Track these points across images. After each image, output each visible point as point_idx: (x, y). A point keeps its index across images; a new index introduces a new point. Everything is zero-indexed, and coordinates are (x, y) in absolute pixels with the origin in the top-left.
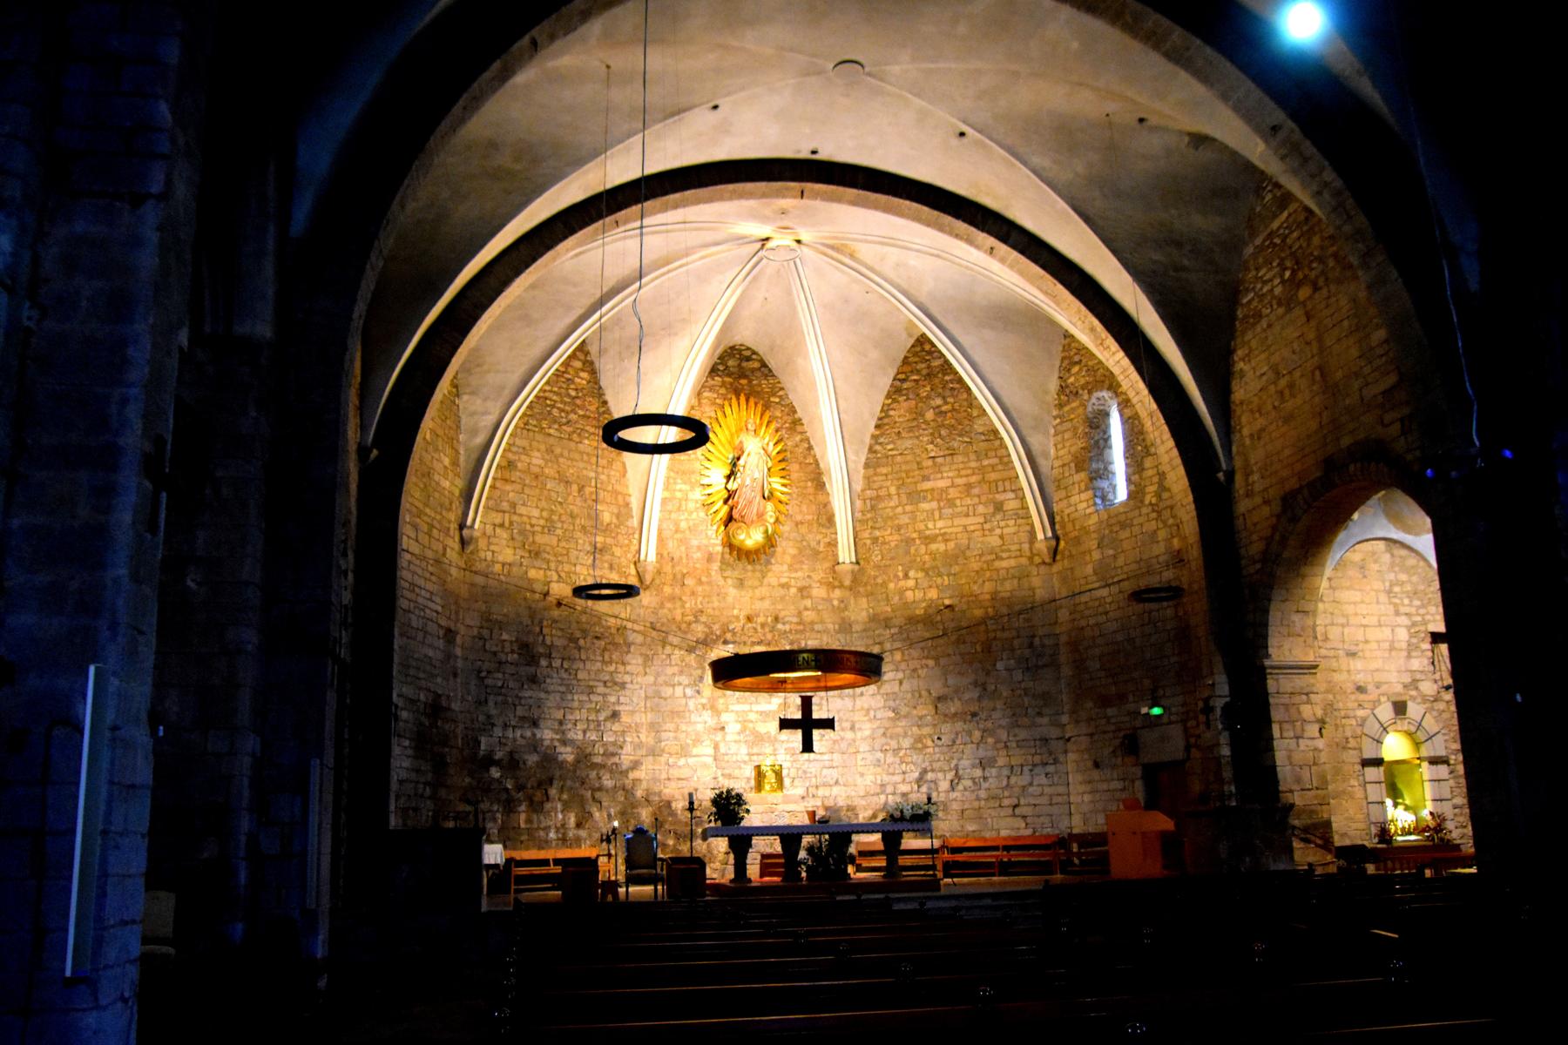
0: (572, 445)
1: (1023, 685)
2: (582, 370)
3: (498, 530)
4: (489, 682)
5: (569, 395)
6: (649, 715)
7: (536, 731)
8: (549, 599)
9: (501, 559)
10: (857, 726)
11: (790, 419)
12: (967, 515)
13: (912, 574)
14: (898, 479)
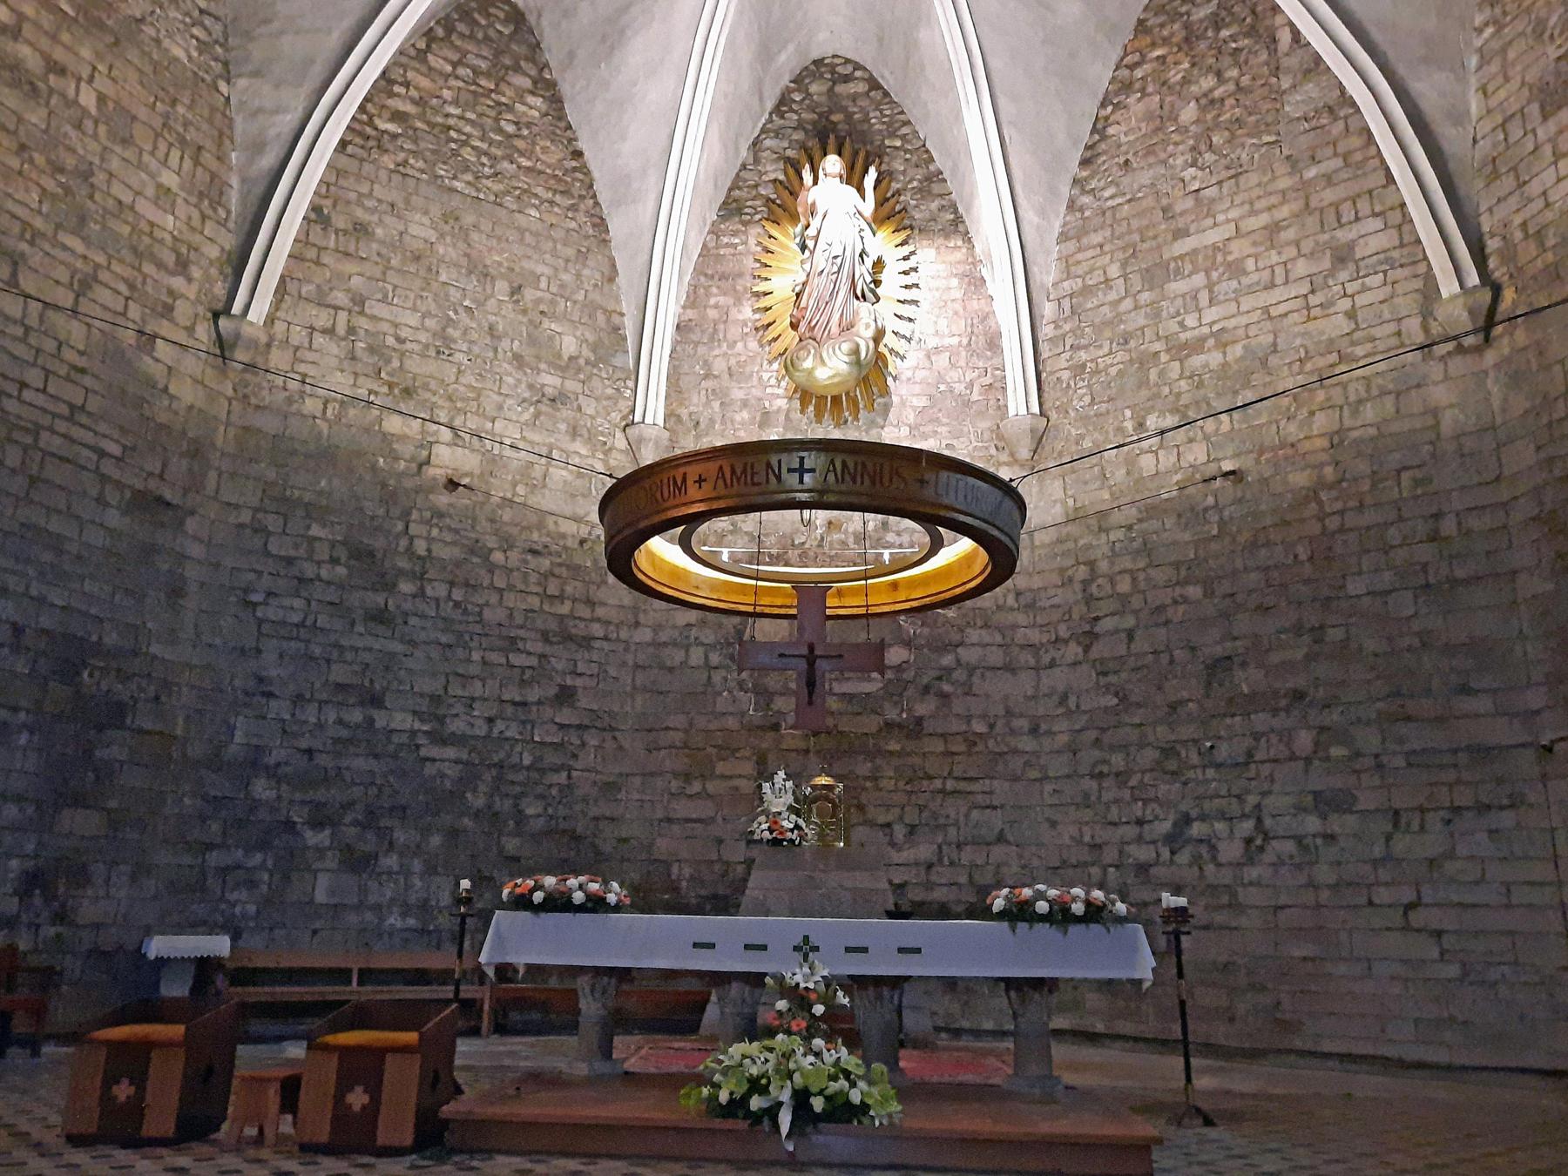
1: (1416, 626)
2: (532, 93)
3: (319, 340)
4: (271, 612)
5: (500, 131)
6: (639, 700)
8: (431, 471)
10: (1044, 727)
11: (919, 174)
12: (1272, 285)
14: (1124, 249)
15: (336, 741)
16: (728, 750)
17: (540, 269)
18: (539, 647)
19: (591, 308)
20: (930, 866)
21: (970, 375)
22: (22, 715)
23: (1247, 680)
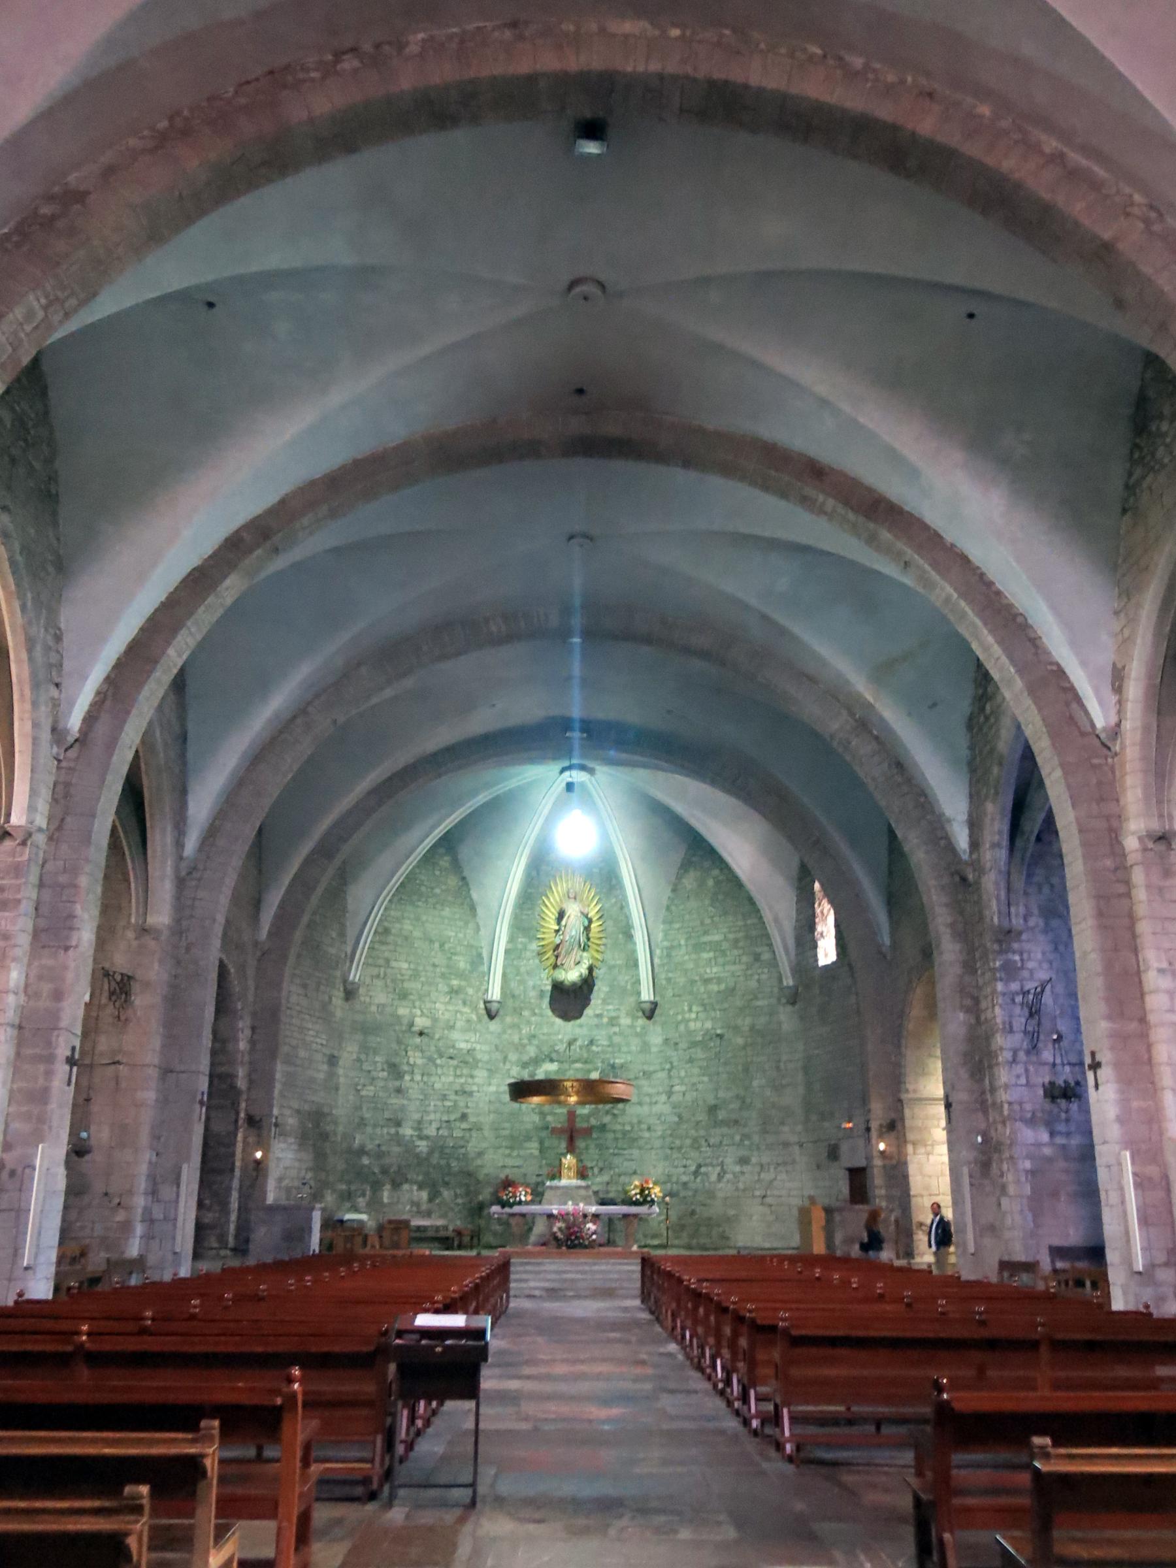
4: (363, 1093)
9: (377, 1001)
12: (735, 963)
13: (695, 1008)
16: (528, 1138)
18: (453, 1097)
19: (470, 946)
20: (608, 1183)
21: (627, 978)
23: (722, 1115)
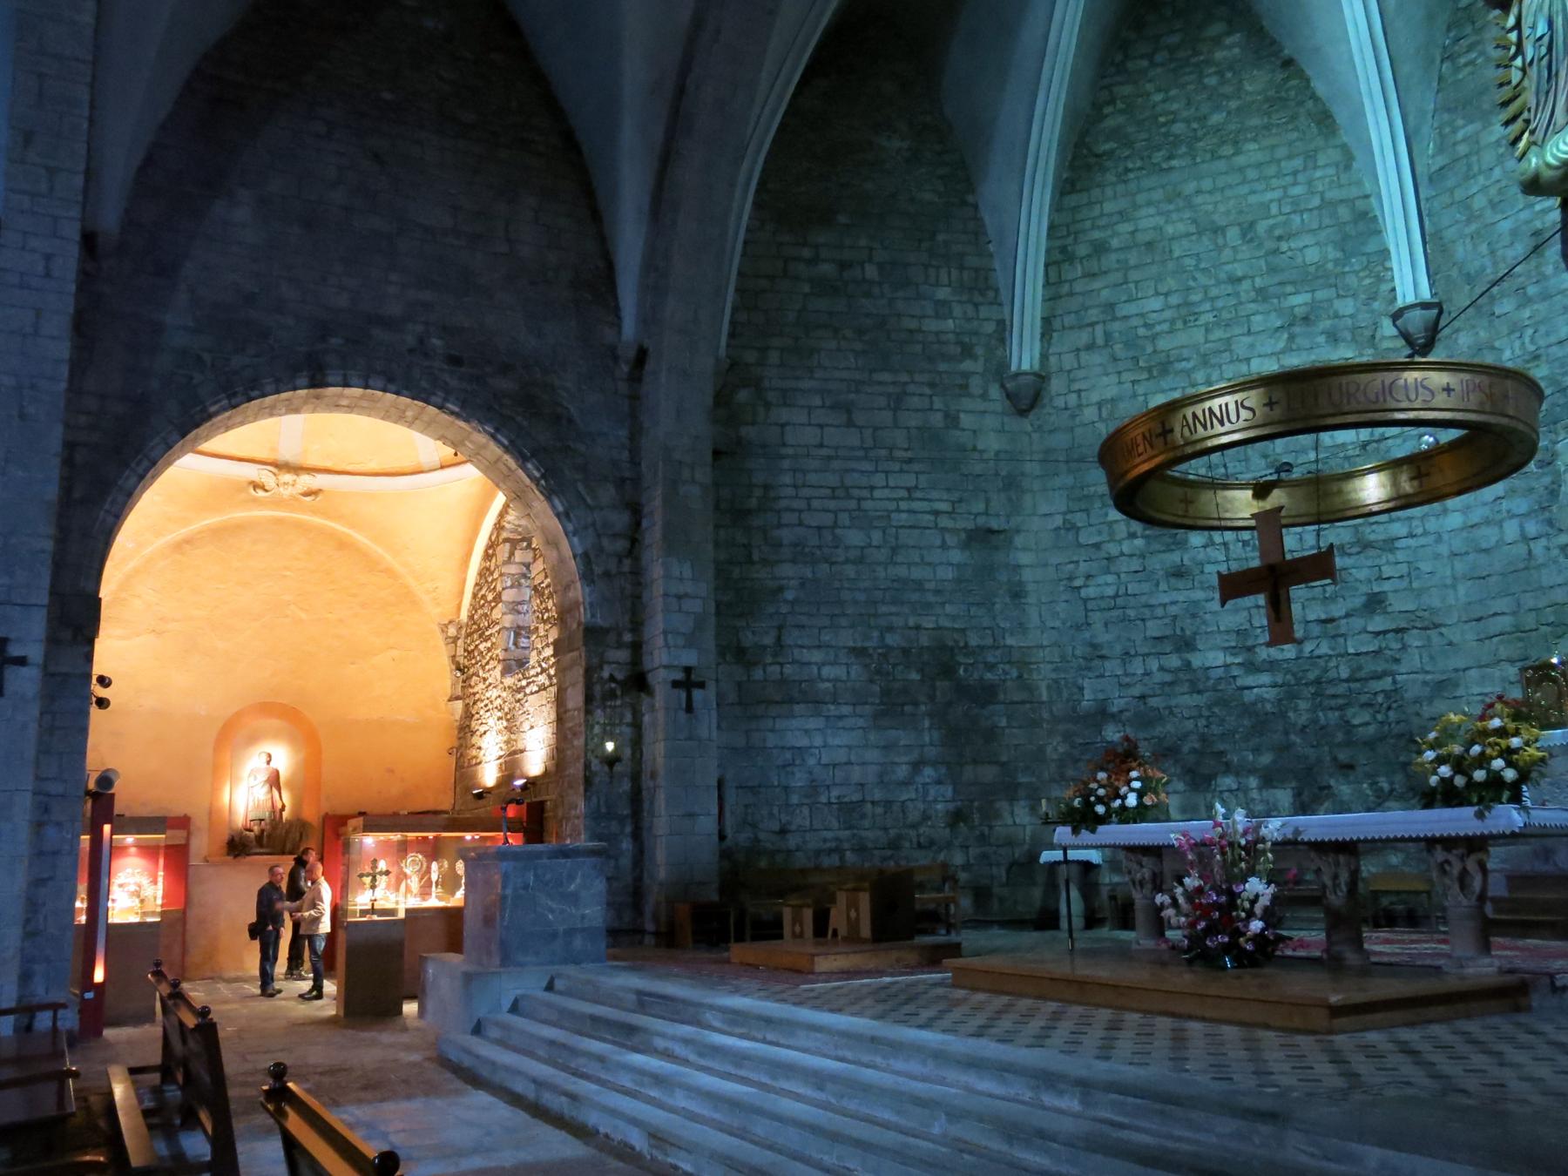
0: (1221, 165)
4: (1091, 592)
6: (1462, 590)
7: (1188, 656)
15: (1163, 684)
17: (1269, 196)
22: (923, 708)
